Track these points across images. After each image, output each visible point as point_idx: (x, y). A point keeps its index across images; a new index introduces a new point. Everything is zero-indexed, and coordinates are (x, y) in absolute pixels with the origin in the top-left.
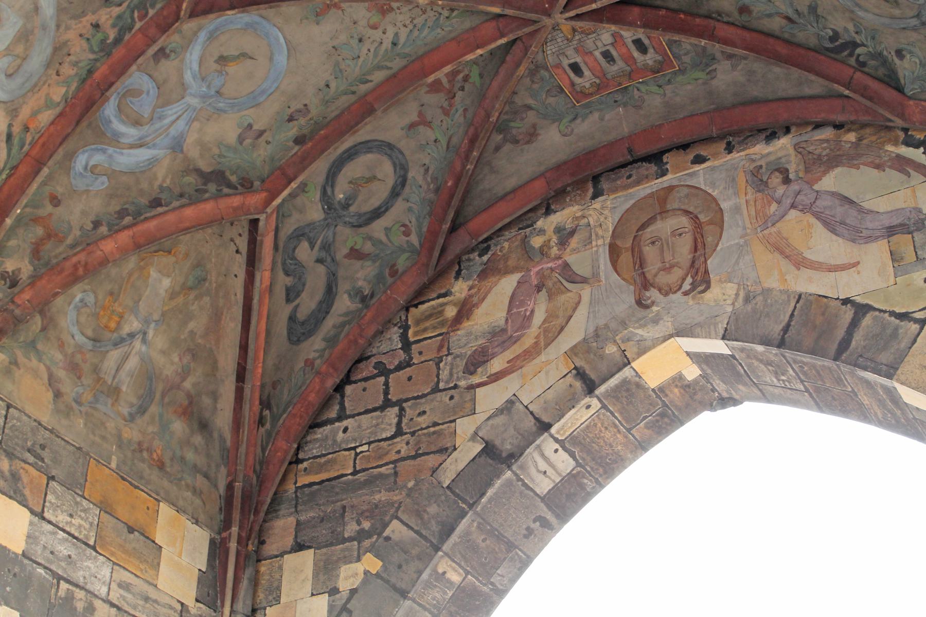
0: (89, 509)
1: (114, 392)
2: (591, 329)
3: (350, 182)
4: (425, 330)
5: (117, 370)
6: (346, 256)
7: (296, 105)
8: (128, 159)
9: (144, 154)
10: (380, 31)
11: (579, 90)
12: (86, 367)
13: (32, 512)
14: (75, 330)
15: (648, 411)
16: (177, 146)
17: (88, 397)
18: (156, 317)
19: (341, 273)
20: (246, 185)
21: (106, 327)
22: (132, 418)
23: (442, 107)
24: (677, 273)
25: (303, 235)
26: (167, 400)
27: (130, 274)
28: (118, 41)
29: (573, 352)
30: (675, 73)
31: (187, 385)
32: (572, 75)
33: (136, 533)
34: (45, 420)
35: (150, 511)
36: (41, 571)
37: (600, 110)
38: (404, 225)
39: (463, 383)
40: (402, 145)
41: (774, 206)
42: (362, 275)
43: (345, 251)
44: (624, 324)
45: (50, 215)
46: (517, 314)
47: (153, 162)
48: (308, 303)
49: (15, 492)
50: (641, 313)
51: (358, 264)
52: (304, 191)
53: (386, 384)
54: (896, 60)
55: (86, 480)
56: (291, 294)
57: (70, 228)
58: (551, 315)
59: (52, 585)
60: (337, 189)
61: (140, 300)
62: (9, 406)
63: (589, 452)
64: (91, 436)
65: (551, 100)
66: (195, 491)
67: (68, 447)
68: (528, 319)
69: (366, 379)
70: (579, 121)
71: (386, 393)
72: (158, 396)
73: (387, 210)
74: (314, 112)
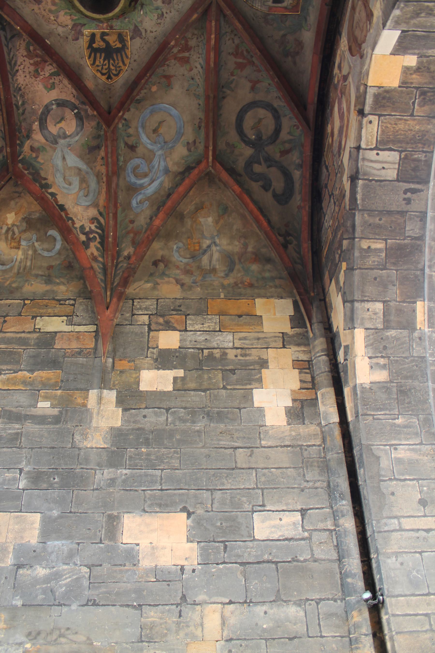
1: (214, 270)
3: (252, 129)
5: (210, 262)
6: (281, 157)
7: (197, 122)
8: (151, 190)
9: (156, 184)
10: (194, 69)
14: (181, 259)
15: (411, 98)
16: (167, 171)
17: (199, 278)
18: (215, 234)
20: (199, 162)
21: (195, 250)
22: (227, 275)
23: (255, 71)
26: (242, 260)
31: (250, 249)
34: (178, 297)
35: (250, 305)
38: (295, 126)
42: (295, 157)
43: (278, 155)
45: (133, 227)
47: (161, 184)
48: (278, 184)
49: (169, 327)
52: (235, 147)
55: (208, 308)
57: (142, 226)
59: (199, 353)
60: (249, 136)
61: (203, 232)
62: (157, 300)
63: (400, 142)
64: (206, 292)
66: (276, 287)
67: (194, 300)
72: (237, 261)
73: (280, 126)
74: (203, 117)
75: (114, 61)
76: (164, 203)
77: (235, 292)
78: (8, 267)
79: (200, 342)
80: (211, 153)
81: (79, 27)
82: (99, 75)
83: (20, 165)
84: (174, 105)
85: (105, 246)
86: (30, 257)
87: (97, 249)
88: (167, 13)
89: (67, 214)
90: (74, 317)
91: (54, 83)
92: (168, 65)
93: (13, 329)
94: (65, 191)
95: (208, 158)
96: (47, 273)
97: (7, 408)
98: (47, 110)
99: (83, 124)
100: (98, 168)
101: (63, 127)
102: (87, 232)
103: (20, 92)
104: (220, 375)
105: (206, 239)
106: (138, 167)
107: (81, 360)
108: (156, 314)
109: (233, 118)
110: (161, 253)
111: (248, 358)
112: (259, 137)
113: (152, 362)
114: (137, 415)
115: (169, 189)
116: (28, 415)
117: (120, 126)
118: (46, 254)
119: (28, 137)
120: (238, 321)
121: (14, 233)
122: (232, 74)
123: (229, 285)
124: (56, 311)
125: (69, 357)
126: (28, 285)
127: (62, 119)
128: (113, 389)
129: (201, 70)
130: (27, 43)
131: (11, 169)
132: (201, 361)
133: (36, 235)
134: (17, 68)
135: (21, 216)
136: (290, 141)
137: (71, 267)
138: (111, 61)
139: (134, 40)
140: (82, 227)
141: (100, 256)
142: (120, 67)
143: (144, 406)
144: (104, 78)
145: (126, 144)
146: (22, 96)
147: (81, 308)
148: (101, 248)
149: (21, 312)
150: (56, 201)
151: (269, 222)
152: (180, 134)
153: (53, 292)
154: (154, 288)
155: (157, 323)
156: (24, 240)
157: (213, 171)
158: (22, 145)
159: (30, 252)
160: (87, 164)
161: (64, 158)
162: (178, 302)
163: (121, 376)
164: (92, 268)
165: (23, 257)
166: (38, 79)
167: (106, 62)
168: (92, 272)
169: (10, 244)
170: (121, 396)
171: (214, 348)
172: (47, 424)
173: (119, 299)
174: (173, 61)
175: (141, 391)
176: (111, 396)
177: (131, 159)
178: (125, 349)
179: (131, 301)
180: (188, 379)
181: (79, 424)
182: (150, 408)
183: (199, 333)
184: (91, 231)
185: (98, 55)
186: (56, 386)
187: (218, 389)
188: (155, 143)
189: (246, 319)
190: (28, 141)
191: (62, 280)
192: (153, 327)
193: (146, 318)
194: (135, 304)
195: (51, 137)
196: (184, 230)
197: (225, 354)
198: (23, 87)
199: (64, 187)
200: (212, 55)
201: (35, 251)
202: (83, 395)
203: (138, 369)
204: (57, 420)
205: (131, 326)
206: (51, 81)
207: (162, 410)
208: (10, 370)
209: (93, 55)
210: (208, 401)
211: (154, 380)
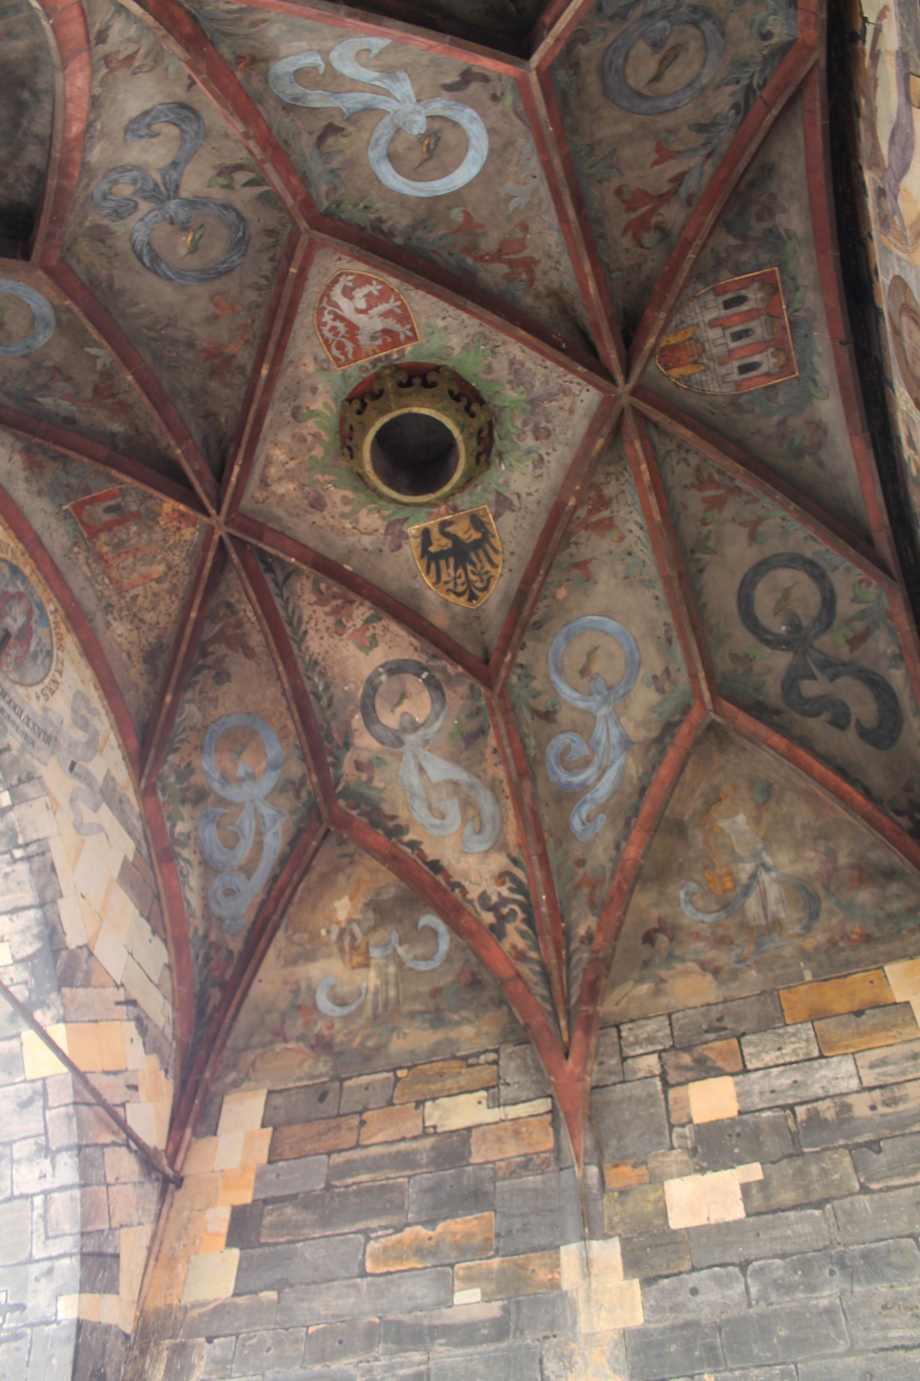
1: (776, 925)
3: (775, 614)
5: (765, 908)
6: (852, 650)
7: (661, 632)
8: (603, 789)
9: (611, 775)
11: (777, 370)
13: (733, 1074)
14: (700, 916)
16: (626, 744)
18: (760, 846)
20: (686, 710)
21: (725, 891)
22: (807, 929)
23: (746, 503)
26: (833, 888)
30: (782, 272)
31: (843, 860)
32: (754, 373)
33: (868, 1012)
34: (712, 998)
35: (876, 983)
36: (765, 1114)
38: (860, 582)
42: (882, 644)
43: (845, 649)
45: (585, 875)
47: (622, 772)
49: (706, 1072)
52: (751, 660)
54: (774, 40)
55: (782, 1010)
56: (840, 720)
57: (603, 867)
59: (786, 1118)
60: (774, 629)
61: (733, 850)
62: (669, 1016)
64: (771, 975)
65: (781, 399)
67: (748, 1000)
70: (817, 378)
72: (822, 893)
73: (832, 591)
74: (670, 620)
75: (474, 565)
76: (636, 810)
77: (833, 962)
78: (353, 1007)
79: (782, 1092)
80: (704, 685)
81: (398, 527)
82: (452, 598)
83: (341, 803)
84: (608, 613)
85: (537, 925)
86: (392, 979)
87: (522, 934)
88: (548, 454)
89: (448, 877)
90: (502, 1087)
91: (374, 635)
92: (576, 544)
93: (380, 1137)
94: (436, 832)
95: (701, 697)
96: (431, 1005)
97: (391, 1317)
98: (372, 686)
99: (443, 695)
100: (491, 771)
101: (407, 710)
102: (496, 904)
103: (318, 669)
104: (847, 1161)
105: (742, 860)
106: (567, 750)
107: (531, 1180)
108: (673, 1047)
109: (732, 604)
110: (655, 913)
111: (901, 1107)
112: (795, 626)
113: (685, 1158)
114: (675, 1290)
115: (640, 779)
116: (436, 1327)
117: (514, 680)
118: (422, 966)
119: (347, 745)
120: (857, 1026)
121: (353, 937)
122: (704, 523)
123: (817, 948)
124: (462, 1083)
125: (504, 1179)
126: (398, 1037)
127: (403, 696)
128: (611, 1237)
129: (640, 534)
130: (314, 580)
131: (325, 814)
132: (794, 1136)
133: (398, 931)
134: (303, 627)
135: (361, 901)
136: (861, 615)
137: (477, 984)
138: (469, 568)
139: (501, 519)
140: (484, 897)
141: (530, 947)
142: (487, 573)
143: (687, 1266)
144: (462, 601)
145: (535, 712)
146: (322, 674)
147: (513, 1065)
148: (530, 932)
149: (392, 1097)
150: (422, 855)
151: (867, 792)
152: (634, 664)
153: (450, 1042)
154: (658, 992)
155: (679, 1067)
156: (376, 946)
157: (718, 719)
158: (338, 764)
159: (392, 969)
161: (421, 770)
162: (714, 1013)
163: (623, 1204)
164: (519, 976)
165: (378, 982)
166: (345, 636)
167: (460, 571)
168: (520, 985)
169: (351, 960)
170: (632, 1250)
171: (817, 1100)
172: (481, 1343)
173: (587, 1031)
174: (583, 533)
175: (675, 1232)
176: (608, 1252)
177: (549, 738)
178: (620, 1139)
179: (614, 1031)
180: (774, 1183)
181: (549, 1333)
182: (702, 1269)
183: (775, 1071)
184: (503, 901)
185: (443, 563)
186: (487, 1250)
187: (851, 1194)
188: (590, 694)
189: (874, 1016)
190: (349, 754)
191: (464, 1013)
192: (672, 1077)
193: (652, 1062)
194: (624, 1034)
196: (692, 854)
197: (845, 1108)
198: (320, 658)
199: (433, 826)
200: (652, 500)
201: (400, 964)
202: (548, 1261)
203: (656, 1180)
204: (500, 1329)
205: (624, 1086)
206: (369, 634)
207: (731, 1268)
208: (386, 1227)
209: (433, 566)
210: (834, 1229)
211: (699, 1199)
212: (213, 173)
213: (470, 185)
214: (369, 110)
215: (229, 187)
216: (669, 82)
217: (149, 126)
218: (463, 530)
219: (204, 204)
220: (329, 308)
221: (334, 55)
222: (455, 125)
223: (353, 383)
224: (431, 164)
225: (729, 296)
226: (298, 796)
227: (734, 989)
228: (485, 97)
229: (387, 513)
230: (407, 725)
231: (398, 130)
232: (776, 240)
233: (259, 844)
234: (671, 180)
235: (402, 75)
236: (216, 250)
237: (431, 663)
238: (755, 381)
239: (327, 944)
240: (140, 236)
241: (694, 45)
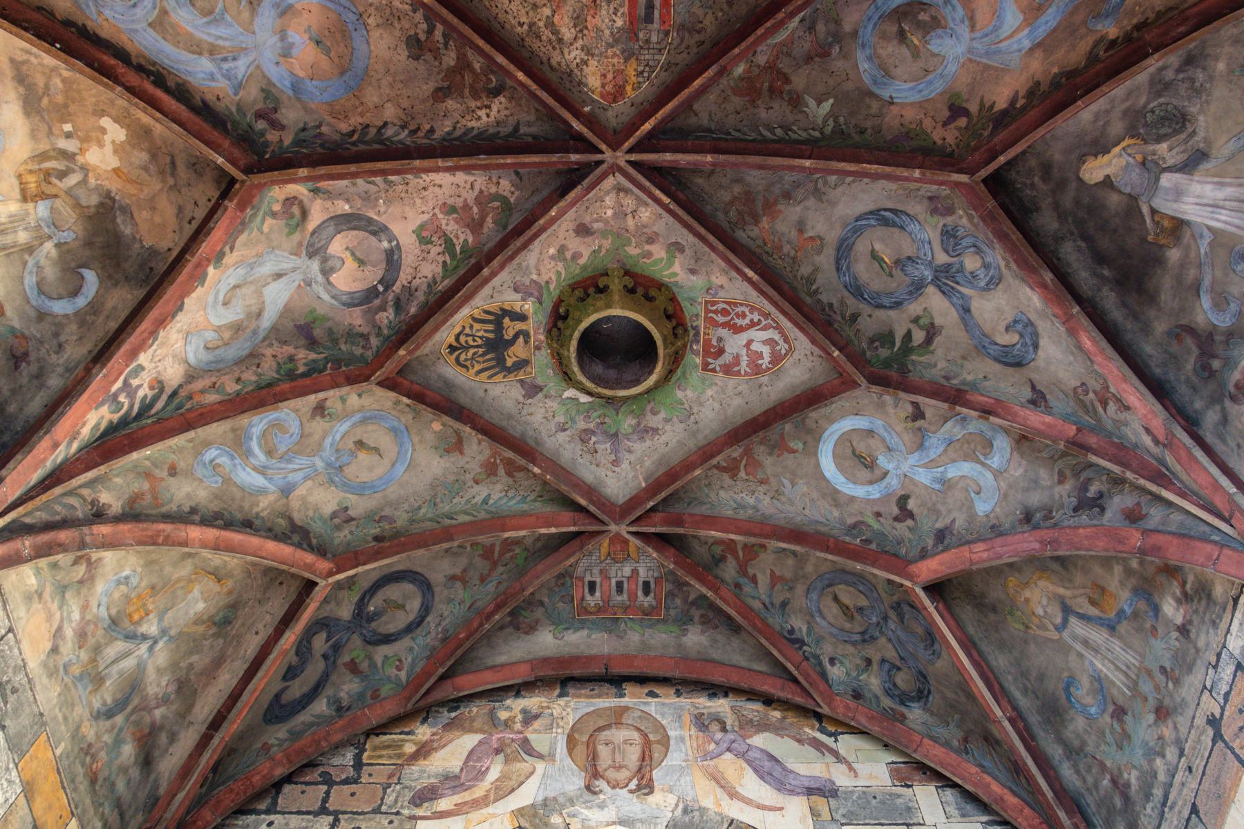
0: (14, 782)
2: (540, 798)
4: (380, 757)
6: (345, 664)
7: (387, 512)
9: (259, 481)
12: (91, 641)
17: (76, 670)
18: (173, 632)
19: (334, 677)
24: (624, 774)
25: (327, 626)
26: (133, 718)
27: (179, 580)
28: (304, 375)
29: (519, 813)
30: (658, 621)
32: (586, 590)
35: (61, 822)
37: (590, 629)
38: (400, 660)
39: (406, 812)
40: (437, 590)
41: (712, 746)
42: (348, 687)
43: (347, 659)
44: (571, 801)
45: (163, 479)
46: (473, 767)
47: (262, 491)
48: (297, 689)
50: (588, 796)
51: (349, 676)
53: (328, 793)
54: (828, 666)
58: (504, 777)
62: (10, 630)
64: (57, 710)
65: (560, 605)
68: (482, 774)
69: (308, 784)
71: (325, 801)
72: (130, 708)
73: (396, 640)
74: (399, 524)
94: (211, 299)
98: (378, 230)
99: (355, 306)
100: (269, 352)
102: (130, 385)
121: (62, 175)
127: (361, 262)
136: (373, 665)
138: (481, 351)
144: (451, 340)
152: (361, 489)
156: (52, 210)
157: (317, 588)
159: (23, 237)
160: (274, 329)
161: (279, 276)
166: (437, 211)
169: (31, 172)
184: (131, 393)
185: (490, 327)
188: (337, 451)
195: (323, 242)
199: (217, 293)
209: (491, 318)
212: (938, 322)
213: (818, 465)
214: (921, 446)
215: (916, 320)
216: (828, 601)
217: (1022, 336)
218: (518, 351)
219: (910, 293)
220: (764, 322)
221: (989, 476)
222: (871, 483)
223: (685, 304)
224: (849, 451)
225: (653, 586)
226: (259, 115)
227: (41, 680)
228: (882, 510)
229: (552, 287)
230: (330, 263)
231: (890, 450)
232: (684, 621)
233: (197, 48)
234: (755, 575)
235: (937, 486)
236: (863, 270)
237: (391, 297)
238: (579, 591)
239: (50, 133)
240: (913, 227)
241: (848, 626)
